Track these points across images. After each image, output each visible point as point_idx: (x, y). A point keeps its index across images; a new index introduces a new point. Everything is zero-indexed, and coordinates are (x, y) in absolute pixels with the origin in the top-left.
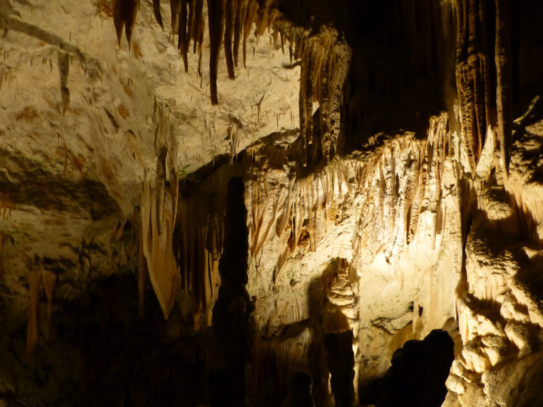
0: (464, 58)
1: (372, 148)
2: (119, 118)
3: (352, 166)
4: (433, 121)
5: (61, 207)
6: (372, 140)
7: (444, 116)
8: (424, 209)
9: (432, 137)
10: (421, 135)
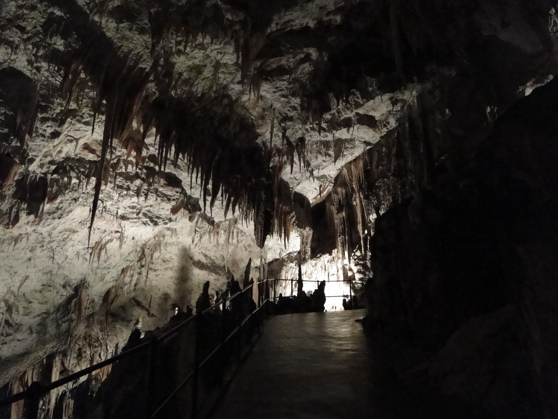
0: (340, 236)
1: (319, 257)
2: (247, 248)
3: (313, 262)
4: (333, 251)
5: (220, 275)
6: (319, 255)
7: (336, 250)
8: (333, 275)
9: (333, 255)
10: (330, 254)
